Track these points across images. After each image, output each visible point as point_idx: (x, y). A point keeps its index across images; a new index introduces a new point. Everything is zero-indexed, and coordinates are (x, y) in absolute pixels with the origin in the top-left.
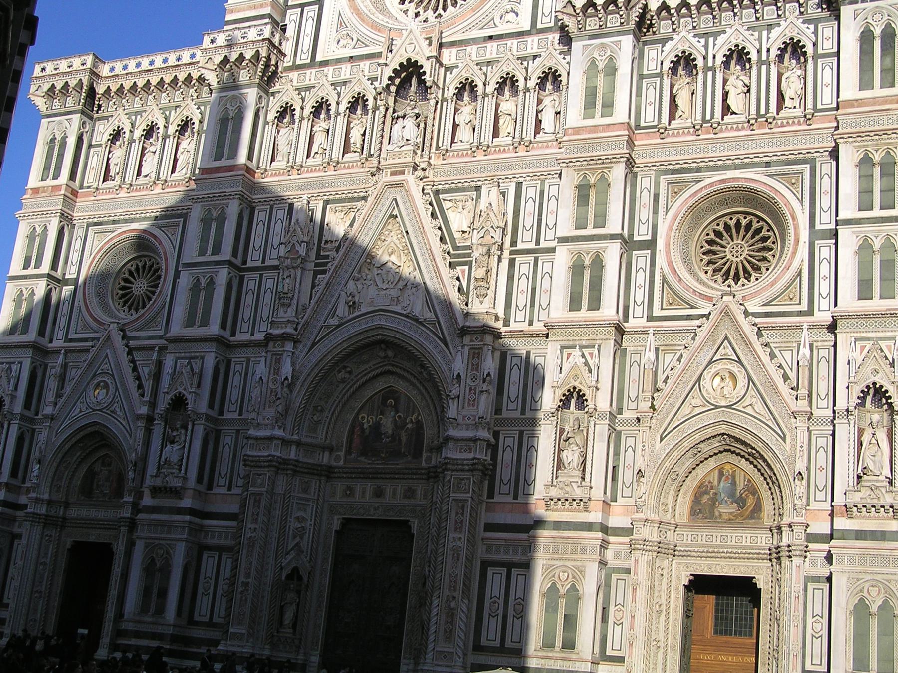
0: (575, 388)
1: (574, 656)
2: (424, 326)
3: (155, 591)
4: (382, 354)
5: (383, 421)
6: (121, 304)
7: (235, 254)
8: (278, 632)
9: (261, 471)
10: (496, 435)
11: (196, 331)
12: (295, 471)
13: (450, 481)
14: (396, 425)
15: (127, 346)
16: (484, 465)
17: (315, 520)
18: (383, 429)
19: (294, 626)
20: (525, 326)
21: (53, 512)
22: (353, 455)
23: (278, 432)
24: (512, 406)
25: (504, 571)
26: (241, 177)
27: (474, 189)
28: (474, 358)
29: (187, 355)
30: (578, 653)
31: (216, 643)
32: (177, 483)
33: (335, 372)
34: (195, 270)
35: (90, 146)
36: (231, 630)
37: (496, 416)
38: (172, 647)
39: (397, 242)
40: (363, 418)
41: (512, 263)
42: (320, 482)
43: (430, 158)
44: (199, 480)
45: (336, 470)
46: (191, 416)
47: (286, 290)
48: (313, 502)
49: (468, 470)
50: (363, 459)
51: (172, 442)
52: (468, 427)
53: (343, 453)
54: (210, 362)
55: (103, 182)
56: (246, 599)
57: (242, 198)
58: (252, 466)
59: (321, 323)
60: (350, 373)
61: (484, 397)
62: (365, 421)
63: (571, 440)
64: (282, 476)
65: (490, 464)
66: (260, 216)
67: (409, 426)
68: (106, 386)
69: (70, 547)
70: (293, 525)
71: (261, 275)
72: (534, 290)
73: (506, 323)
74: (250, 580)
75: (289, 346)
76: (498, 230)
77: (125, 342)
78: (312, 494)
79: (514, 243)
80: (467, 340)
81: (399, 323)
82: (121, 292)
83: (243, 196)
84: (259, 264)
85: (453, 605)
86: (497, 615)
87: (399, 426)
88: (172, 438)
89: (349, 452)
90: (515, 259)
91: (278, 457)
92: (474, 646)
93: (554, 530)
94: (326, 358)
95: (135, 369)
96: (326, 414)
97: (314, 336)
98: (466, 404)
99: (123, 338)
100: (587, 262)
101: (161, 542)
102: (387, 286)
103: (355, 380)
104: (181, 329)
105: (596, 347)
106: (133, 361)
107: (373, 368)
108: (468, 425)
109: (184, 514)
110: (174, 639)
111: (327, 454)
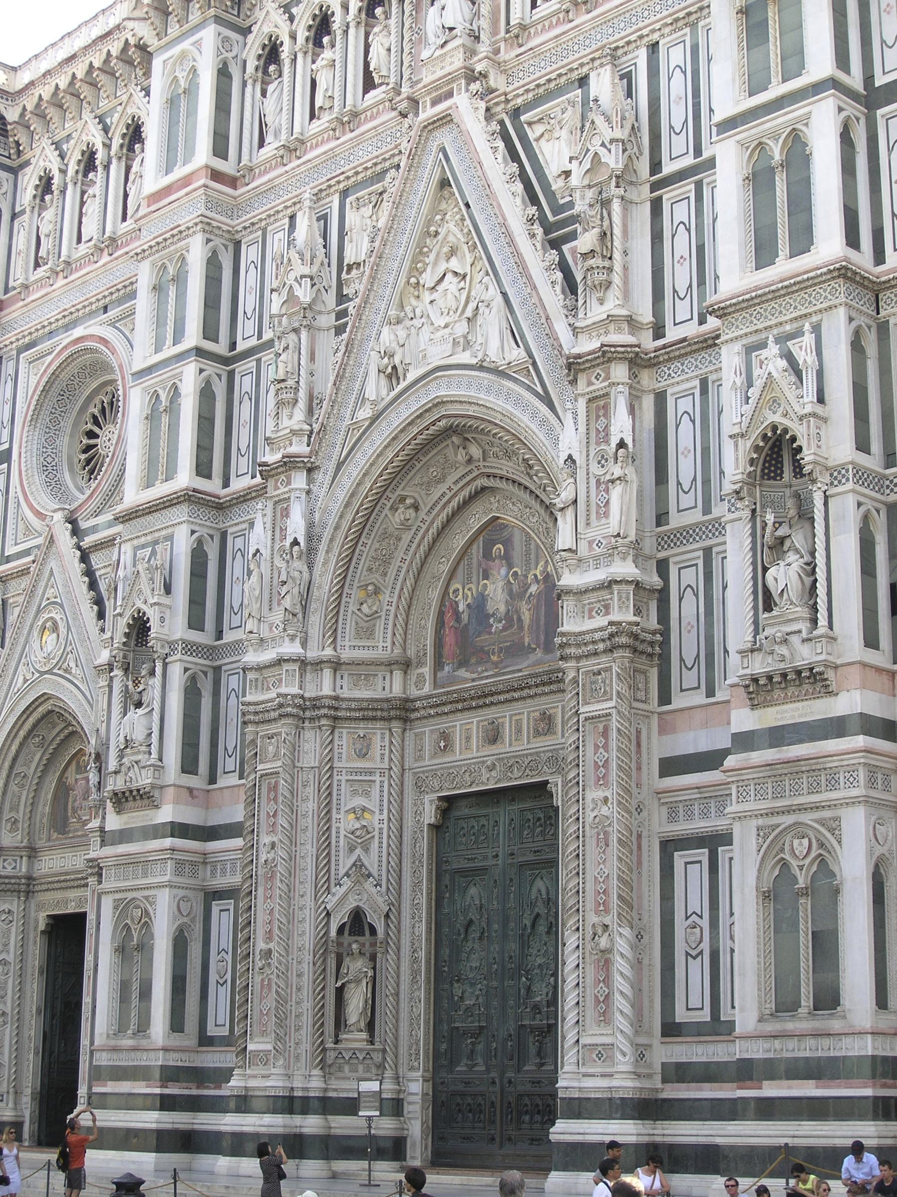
0: (774, 428)
1: (836, 1025)
2: (515, 380)
3: (135, 986)
4: (461, 456)
5: (490, 590)
6: (86, 478)
7: (210, 331)
8: (337, 1042)
9: (272, 728)
10: (662, 567)
11: (161, 490)
12: (335, 718)
13: (575, 681)
14: (510, 593)
15: (79, 548)
16: (636, 637)
17: (390, 811)
18: (490, 608)
19: (371, 1027)
20: (692, 330)
21: (9, 869)
22: (447, 668)
23: (293, 649)
24: (687, 501)
25: (703, 854)
26: (202, 191)
27: (577, 84)
28: (598, 417)
29: (149, 538)
30: (844, 1017)
31: (225, 1075)
32: (144, 779)
33: (386, 511)
34: (150, 381)
35: (14, 216)
36: (251, 1047)
37: (660, 529)
38: (167, 1091)
39: (456, 230)
40: (456, 591)
41: (656, 206)
42: (391, 734)
43: (497, 51)
44: (189, 766)
45: (418, 704)
46: (158, 647)
47: (281, 375)
48: (382, 774)
49: (605, 652)
50: (463, 673)
51: (139, 705)
52: (597, 562)
53: (427, 669)
54: (183, 544)
55: (35, 269)
56: (269, 984)
57: (208, 227)
58: (257, 723)
59: (348, 422)
60: (416, 507)
61: (616, 492)
62: (460, 597)
63: (787, 543)
64: (312, 732)
65: (654, 633)
66: (250, 254)
67: (533, 589)
68: (55, 628)
69: (43, 928)
70: (344, 823)
71: (259, 361)
72: (701, 249)
73: (659, 331)
74: (271, 945)
75: (299, 480)
76: (613, 148)
77: (75, 540)
78: (378, 759)
79: (655, 167)
80: (582, 385)
81: (469, 387)
82: (83, 457)
83: (209, 224)
84: (253, 342)
85: (603, 942)
86: (701, 953)
87: (514, 596)
88: (136, 697)
89: (438, 664)
90: (660, 198)
91: (294, 696)
92: (663, 1025)
93: (771, 746)
94: (362, 488)
95: (93, 585)
96: (385, 597)
97: (338, 449)
98: (593, 516)
99: (76, 532)
100: (777, 155)
101: (134, 894)
102: (447, 319)
103: (429, 519)
104: (137, 494)
105: (807, 327)
106: (89, 573)
107: (456, 489)
108: (596, 558)
109: (164, 836)
110: (170, 1074)
111: (398, 675)
